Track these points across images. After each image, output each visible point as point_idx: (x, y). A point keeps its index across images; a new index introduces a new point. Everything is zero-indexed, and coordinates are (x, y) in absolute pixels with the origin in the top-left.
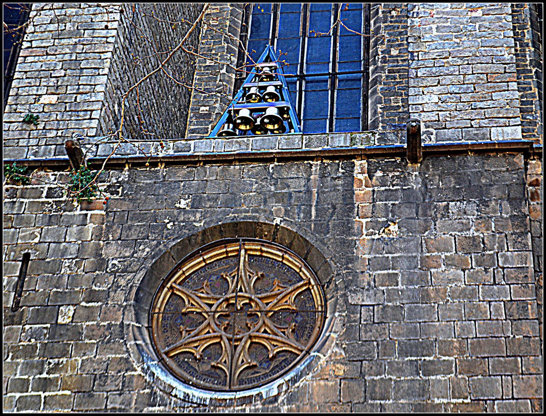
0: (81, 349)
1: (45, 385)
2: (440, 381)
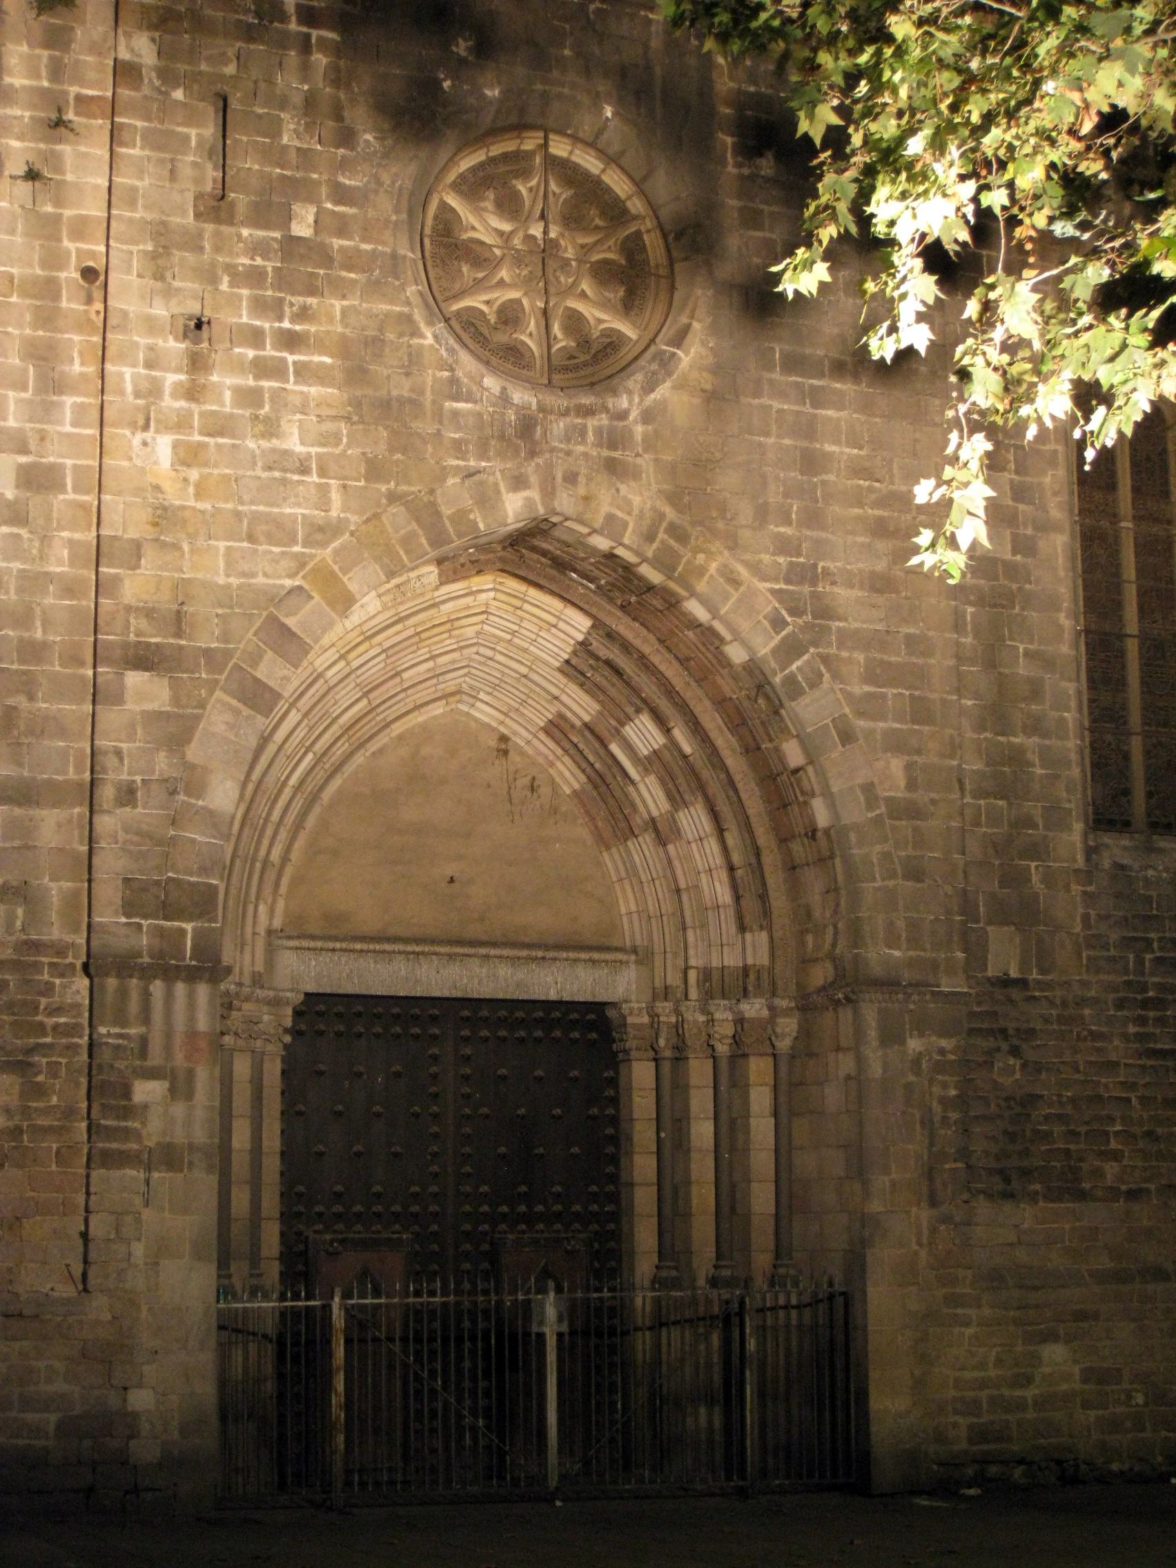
0: (341, 287)
1: (291, 341)
2: (830, 419)
